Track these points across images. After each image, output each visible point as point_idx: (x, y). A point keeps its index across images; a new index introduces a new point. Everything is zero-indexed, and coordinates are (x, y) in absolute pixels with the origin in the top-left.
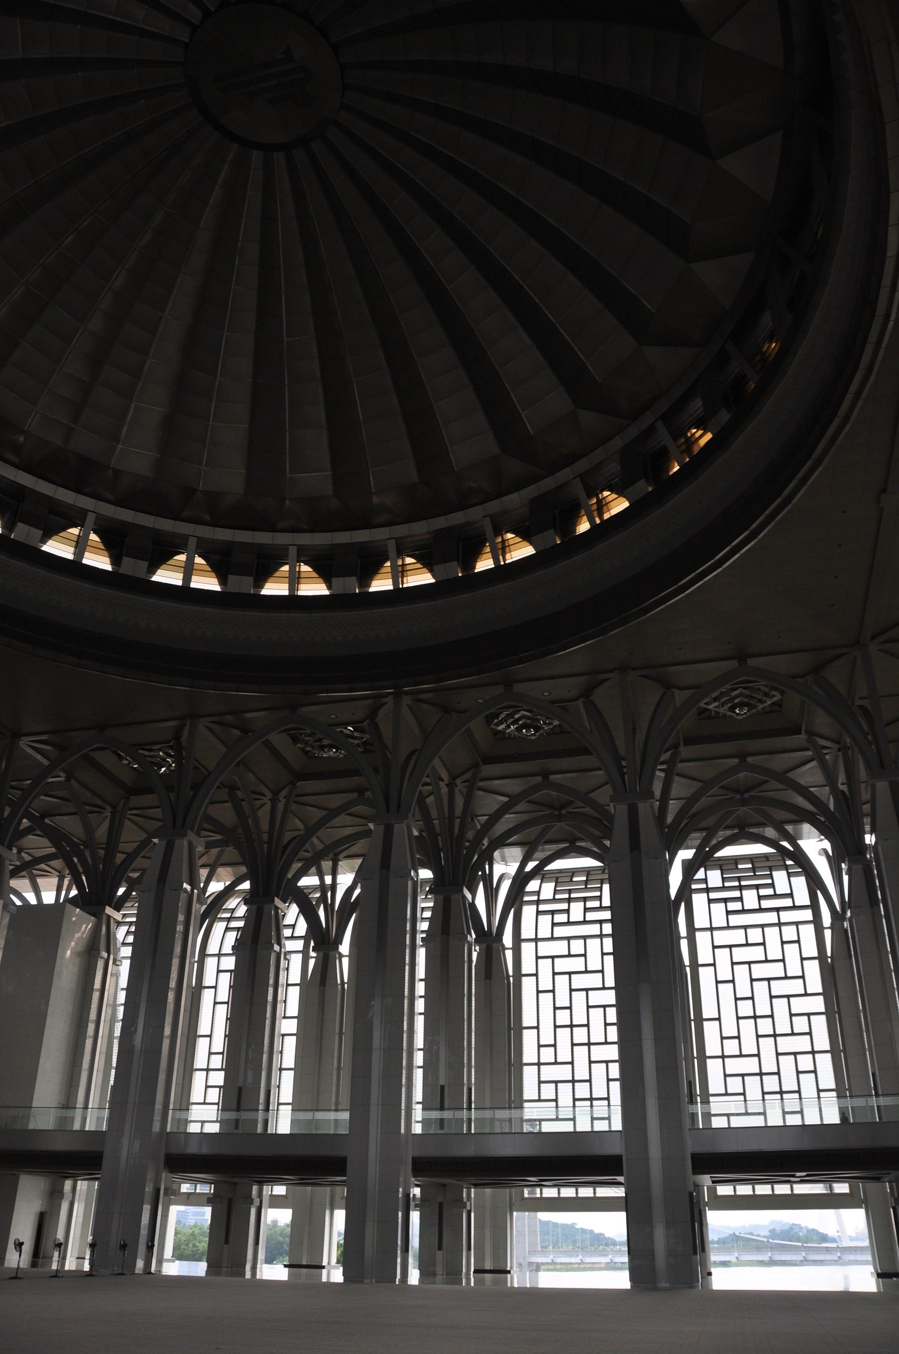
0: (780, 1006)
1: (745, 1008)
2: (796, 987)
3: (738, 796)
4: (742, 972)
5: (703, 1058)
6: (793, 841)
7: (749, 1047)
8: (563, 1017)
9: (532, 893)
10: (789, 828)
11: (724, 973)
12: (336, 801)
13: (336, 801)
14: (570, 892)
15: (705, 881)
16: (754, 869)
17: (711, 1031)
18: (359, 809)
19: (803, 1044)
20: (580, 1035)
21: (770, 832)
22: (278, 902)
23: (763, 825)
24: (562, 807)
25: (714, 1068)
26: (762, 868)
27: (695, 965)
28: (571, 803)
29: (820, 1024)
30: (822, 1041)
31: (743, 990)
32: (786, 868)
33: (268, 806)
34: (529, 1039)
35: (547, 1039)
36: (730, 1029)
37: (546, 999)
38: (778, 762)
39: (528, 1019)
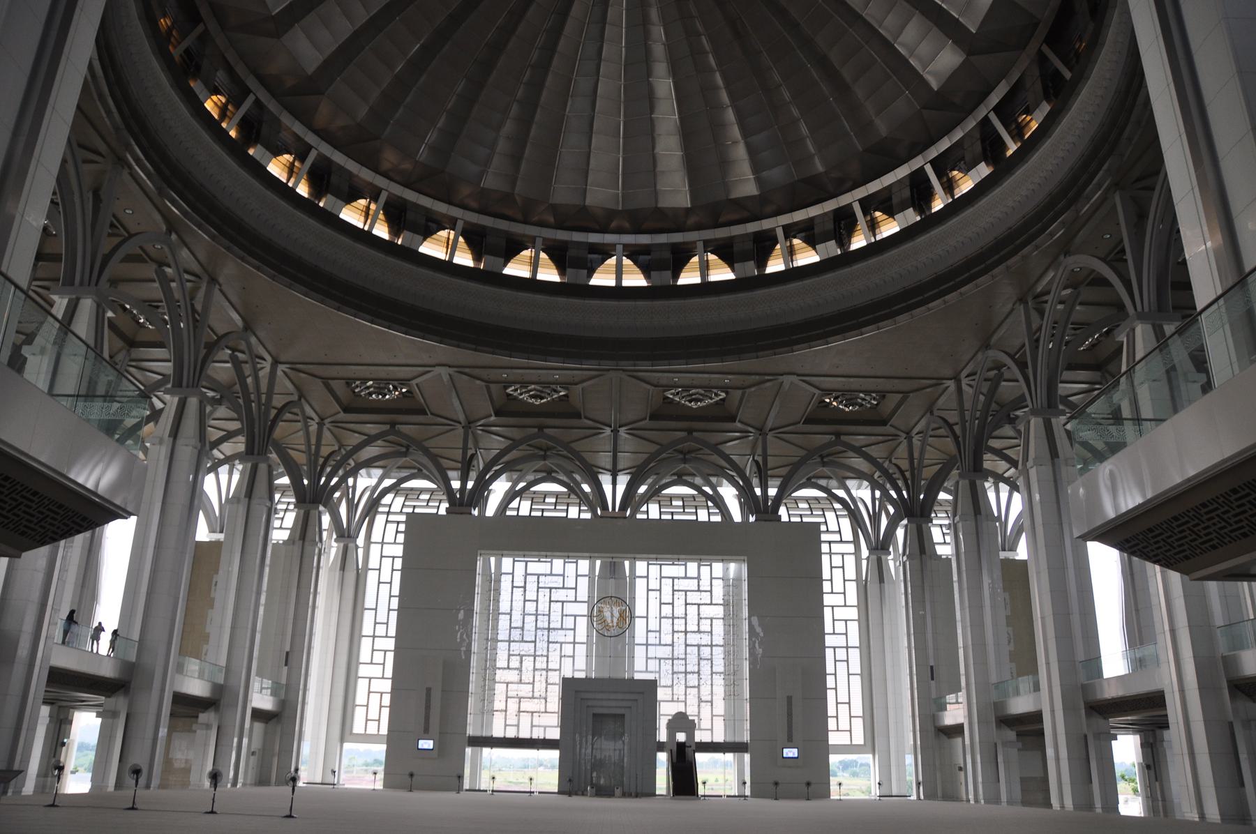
0: (692, 610)
1: (667, 610)
2: (706, 598)
3: (681, 456)
4: (667, 584)
5: (633, 644)
6: (714, 488)
7: (667, 639)
8: (531, 607)
9: (513, 509)
10: (714, 480)
11: (654, 584)
12: (372, 429)
13: (372, 429)
14: (543, 510)
15: (647, 512)
16: (684, 507)
17: (640, 625)
18: (390, 438)
19: (706, 639)
20: (543, 622)
21: (698, 481)
22: (321, 508)
23: (694, 475)
24: (549, 449)
25: (639, 652)
26: (690, 507)
27: (633, 576)
28: (554, 448)
29: (719, 627)
30: (719, 639)
31: (667, 598)
32: (708, 508)
33: (316, 426)
34: (503, 622)
35: (517, 622)
36: (653, 625)
37: (518, 593)
38: (714, 438)
39: (504, 606)
